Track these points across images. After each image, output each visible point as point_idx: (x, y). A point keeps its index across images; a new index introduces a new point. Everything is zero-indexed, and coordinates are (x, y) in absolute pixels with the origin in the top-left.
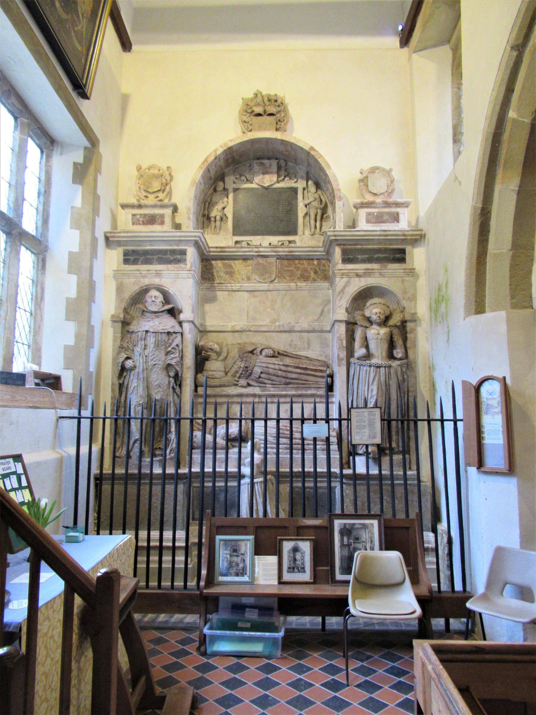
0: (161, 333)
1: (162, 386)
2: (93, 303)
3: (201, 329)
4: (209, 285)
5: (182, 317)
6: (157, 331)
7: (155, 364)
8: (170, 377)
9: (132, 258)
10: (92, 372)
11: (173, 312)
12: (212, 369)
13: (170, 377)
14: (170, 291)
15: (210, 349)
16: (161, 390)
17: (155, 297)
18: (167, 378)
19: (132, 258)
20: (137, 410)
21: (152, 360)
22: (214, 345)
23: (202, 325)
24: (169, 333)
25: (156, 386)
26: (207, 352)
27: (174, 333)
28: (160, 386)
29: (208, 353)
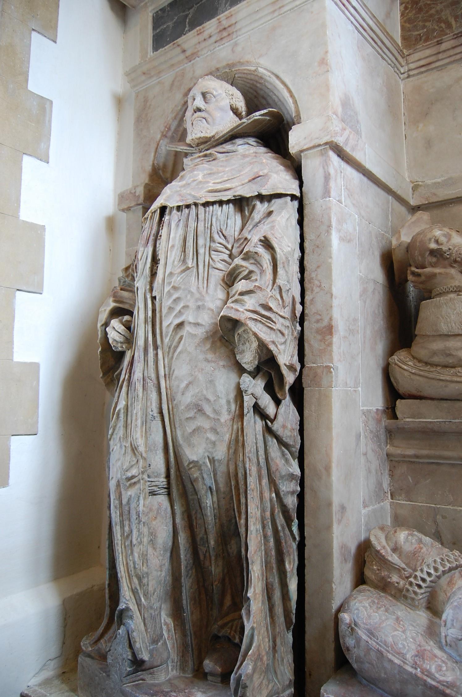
0: (206, 204)
1: (208, 410)
2: (28, 162)
3: (413, 203)
4: (428, 52)
5: (296, 140)
6: (190, 201)
7: (180, 325)
8: (241, 370)
9: (170, 24)
10: (35, 366)
11: (273, 134)
12: (444, 328)
13: (241, 370)
14: (261, 70)
15: (433, 252)
16: (206, 425)
17: (204, 95)
18: (233, 378)
19: (170, 24)
20: (124, 501)
21: (171, 309)
22: (449, 237)
23: (415, 188)
24: (241, 203)
25: (188, 407)
26: (423, 267)
27: (261, 198)
28: (200, 411)
29: (429, 270)
